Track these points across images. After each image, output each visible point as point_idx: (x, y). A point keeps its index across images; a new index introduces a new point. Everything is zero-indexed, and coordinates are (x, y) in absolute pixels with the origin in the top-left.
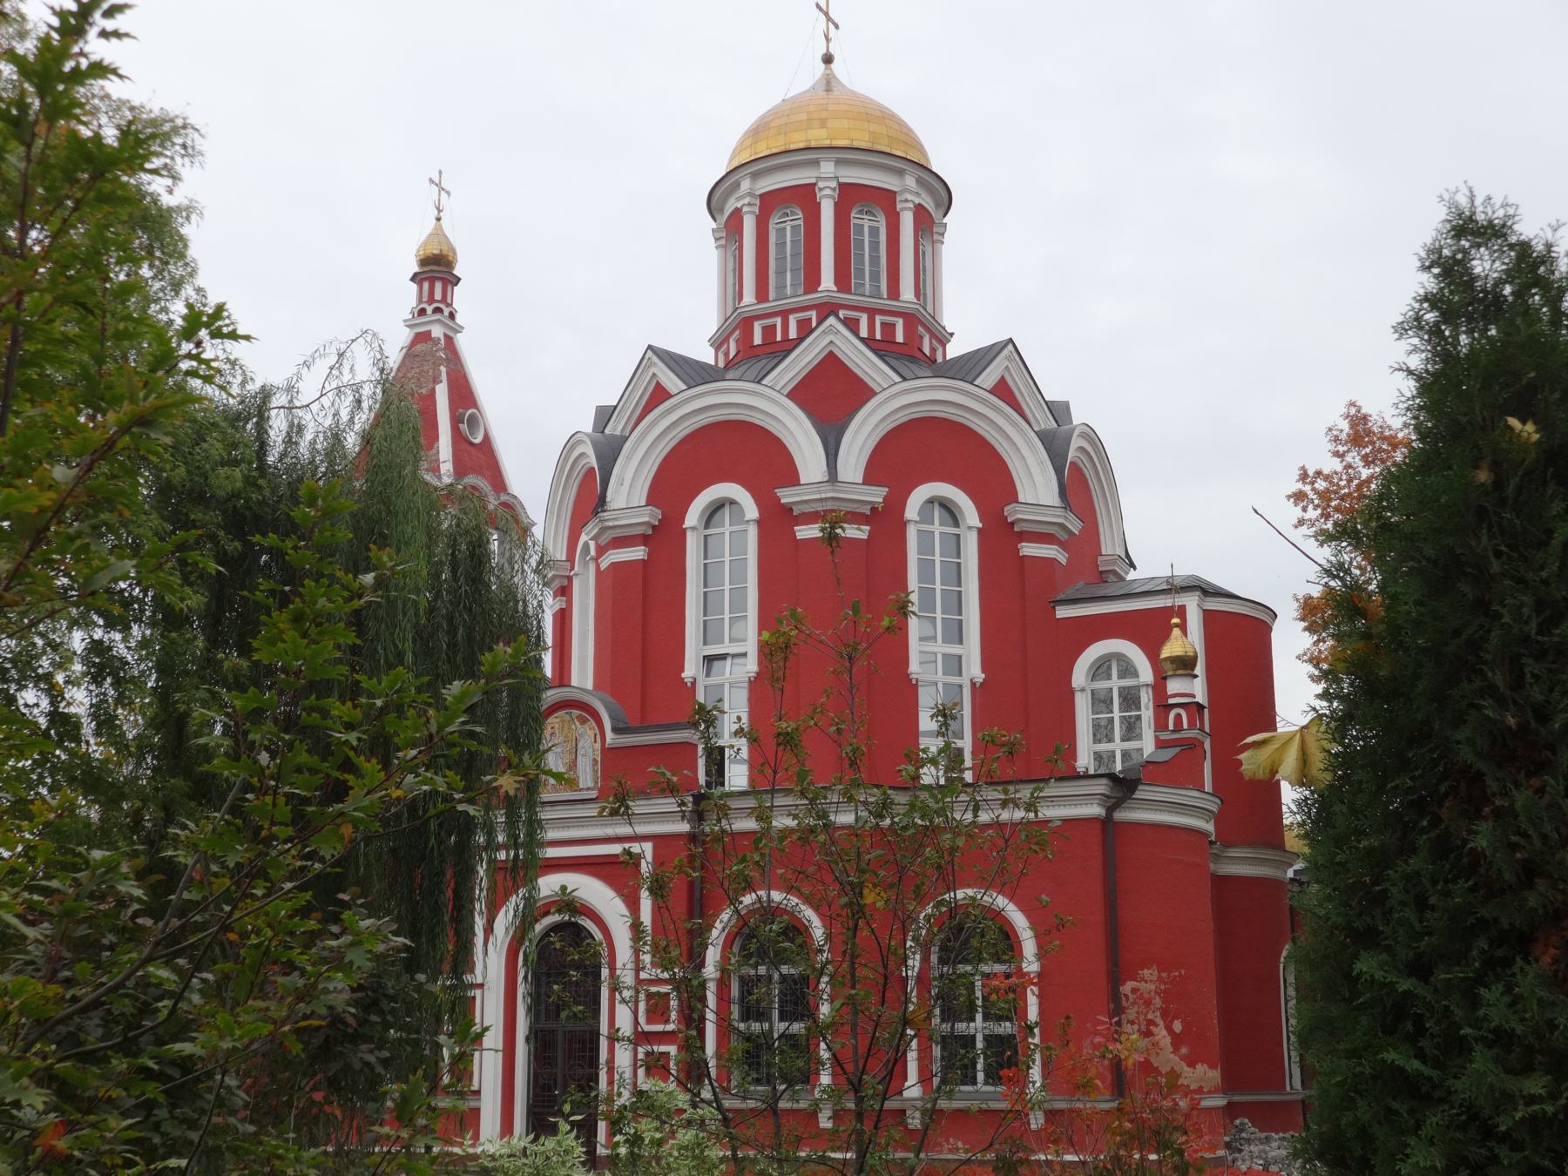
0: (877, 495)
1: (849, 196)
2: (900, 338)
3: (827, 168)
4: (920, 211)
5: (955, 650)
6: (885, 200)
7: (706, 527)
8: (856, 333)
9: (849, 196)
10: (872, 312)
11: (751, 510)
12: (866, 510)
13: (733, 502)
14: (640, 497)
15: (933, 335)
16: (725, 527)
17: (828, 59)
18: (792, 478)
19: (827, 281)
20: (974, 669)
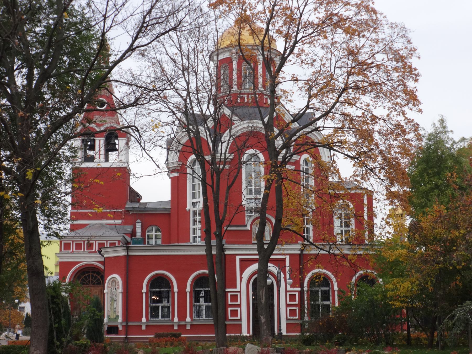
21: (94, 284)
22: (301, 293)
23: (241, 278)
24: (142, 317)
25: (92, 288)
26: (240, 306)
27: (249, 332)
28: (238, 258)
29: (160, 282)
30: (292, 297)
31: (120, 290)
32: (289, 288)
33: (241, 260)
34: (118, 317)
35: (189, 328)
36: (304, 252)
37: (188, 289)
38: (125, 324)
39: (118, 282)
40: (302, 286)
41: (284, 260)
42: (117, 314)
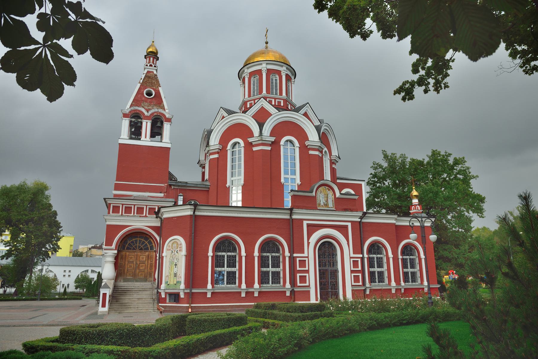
0: (273, 139)
1: (269, 71)
2: (282, 105)
3: (264, 65)
4: (287, 75)
5: (293, 177)
6: (279, 72)
7: (233, 148)
8: (271, 104)
9: (269, 71)
10: (275, 99)
11: (242, 144)
12: (270, 143)
13: (239, 143)
14: (217, 142)
15: (291, 105)
16: (237, 149)
17: (267, 43)
18: (252, 135)
19: (264, 91)
20: (298, 181)
21: (141, 249)
22: (362, 259)
23: (308, 243)
24: (207, 283)
25: (139, 254)
26: (307, 271)
27: (317, 300)
28: (305, 223)
29: (226, 244)
30: (355, 263)
31: (184, 252)
32: (352, 255)
33: (308, 225)
34: (179, 282)
35: (244, 296)
36: (363, 221)
37: (256, 254)
38: (188, 291)
39: (181, 244)
40: (362, 253)
41: (346, 227)
42: (178, 280)
